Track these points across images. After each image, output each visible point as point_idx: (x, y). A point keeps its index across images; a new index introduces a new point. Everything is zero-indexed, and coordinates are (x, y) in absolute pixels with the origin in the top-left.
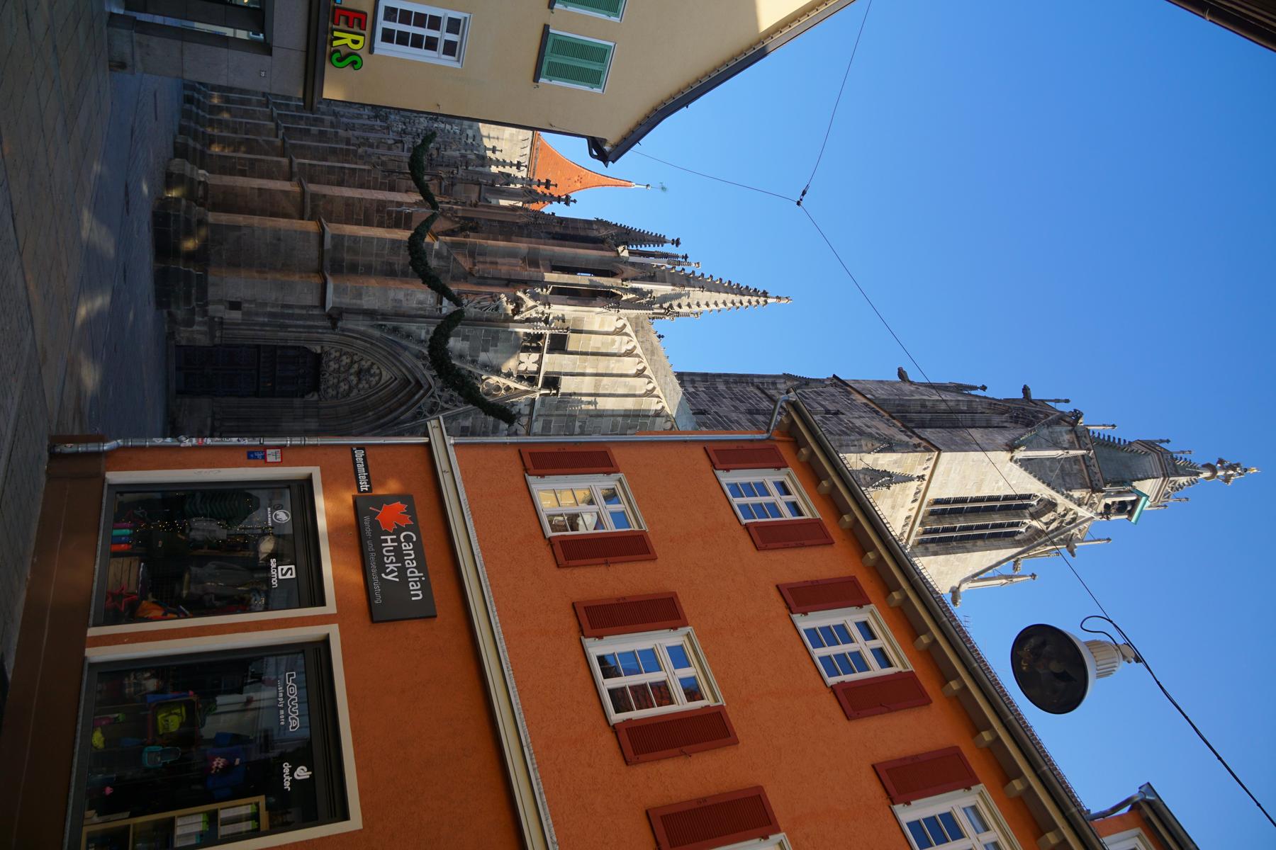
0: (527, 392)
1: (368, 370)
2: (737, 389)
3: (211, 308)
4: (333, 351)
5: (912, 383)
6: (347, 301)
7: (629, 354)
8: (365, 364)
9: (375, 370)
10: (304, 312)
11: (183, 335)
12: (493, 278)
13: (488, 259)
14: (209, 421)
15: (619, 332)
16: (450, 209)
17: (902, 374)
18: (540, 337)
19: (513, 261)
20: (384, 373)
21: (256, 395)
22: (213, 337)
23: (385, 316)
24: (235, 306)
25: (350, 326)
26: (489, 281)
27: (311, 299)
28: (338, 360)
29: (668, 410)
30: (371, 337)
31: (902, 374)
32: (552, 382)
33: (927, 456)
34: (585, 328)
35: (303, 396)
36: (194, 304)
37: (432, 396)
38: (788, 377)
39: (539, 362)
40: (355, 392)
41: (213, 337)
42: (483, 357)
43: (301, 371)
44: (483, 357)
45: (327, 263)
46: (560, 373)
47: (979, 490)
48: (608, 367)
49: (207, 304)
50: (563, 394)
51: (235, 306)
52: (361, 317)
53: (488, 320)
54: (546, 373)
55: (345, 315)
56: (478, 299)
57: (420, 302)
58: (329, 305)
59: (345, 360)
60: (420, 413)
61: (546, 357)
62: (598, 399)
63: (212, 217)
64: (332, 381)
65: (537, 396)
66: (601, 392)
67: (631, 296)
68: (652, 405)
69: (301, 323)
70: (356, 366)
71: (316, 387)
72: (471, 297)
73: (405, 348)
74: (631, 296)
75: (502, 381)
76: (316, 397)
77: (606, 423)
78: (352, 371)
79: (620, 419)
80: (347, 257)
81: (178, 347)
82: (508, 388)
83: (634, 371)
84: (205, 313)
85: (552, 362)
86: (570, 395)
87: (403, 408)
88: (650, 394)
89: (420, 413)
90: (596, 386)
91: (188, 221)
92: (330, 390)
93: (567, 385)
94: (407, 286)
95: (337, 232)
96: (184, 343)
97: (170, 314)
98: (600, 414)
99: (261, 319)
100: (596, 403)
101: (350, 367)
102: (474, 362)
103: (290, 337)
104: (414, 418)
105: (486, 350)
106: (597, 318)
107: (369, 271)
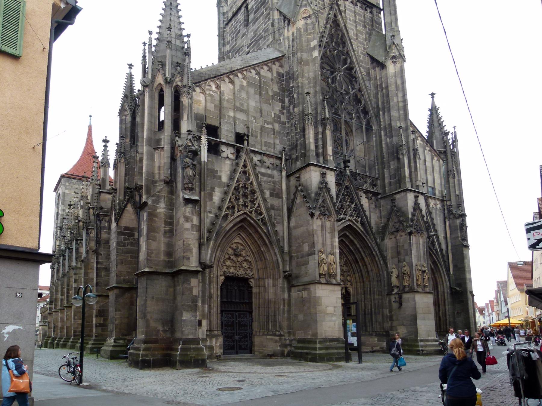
1: (234, 250)
2: (228, 38)
8: (231, 252)
9: (234, 246)
11: (218, 351)
20: (236, 241)
28: (228, 267)
37: (251, 212)
40: (247, 258)
59: (228, 263)
60: (262, 220)
70: (232, 257)
78: (235, 259)
84: (204, 340)
87: (259, 230)
89: (262, 220)
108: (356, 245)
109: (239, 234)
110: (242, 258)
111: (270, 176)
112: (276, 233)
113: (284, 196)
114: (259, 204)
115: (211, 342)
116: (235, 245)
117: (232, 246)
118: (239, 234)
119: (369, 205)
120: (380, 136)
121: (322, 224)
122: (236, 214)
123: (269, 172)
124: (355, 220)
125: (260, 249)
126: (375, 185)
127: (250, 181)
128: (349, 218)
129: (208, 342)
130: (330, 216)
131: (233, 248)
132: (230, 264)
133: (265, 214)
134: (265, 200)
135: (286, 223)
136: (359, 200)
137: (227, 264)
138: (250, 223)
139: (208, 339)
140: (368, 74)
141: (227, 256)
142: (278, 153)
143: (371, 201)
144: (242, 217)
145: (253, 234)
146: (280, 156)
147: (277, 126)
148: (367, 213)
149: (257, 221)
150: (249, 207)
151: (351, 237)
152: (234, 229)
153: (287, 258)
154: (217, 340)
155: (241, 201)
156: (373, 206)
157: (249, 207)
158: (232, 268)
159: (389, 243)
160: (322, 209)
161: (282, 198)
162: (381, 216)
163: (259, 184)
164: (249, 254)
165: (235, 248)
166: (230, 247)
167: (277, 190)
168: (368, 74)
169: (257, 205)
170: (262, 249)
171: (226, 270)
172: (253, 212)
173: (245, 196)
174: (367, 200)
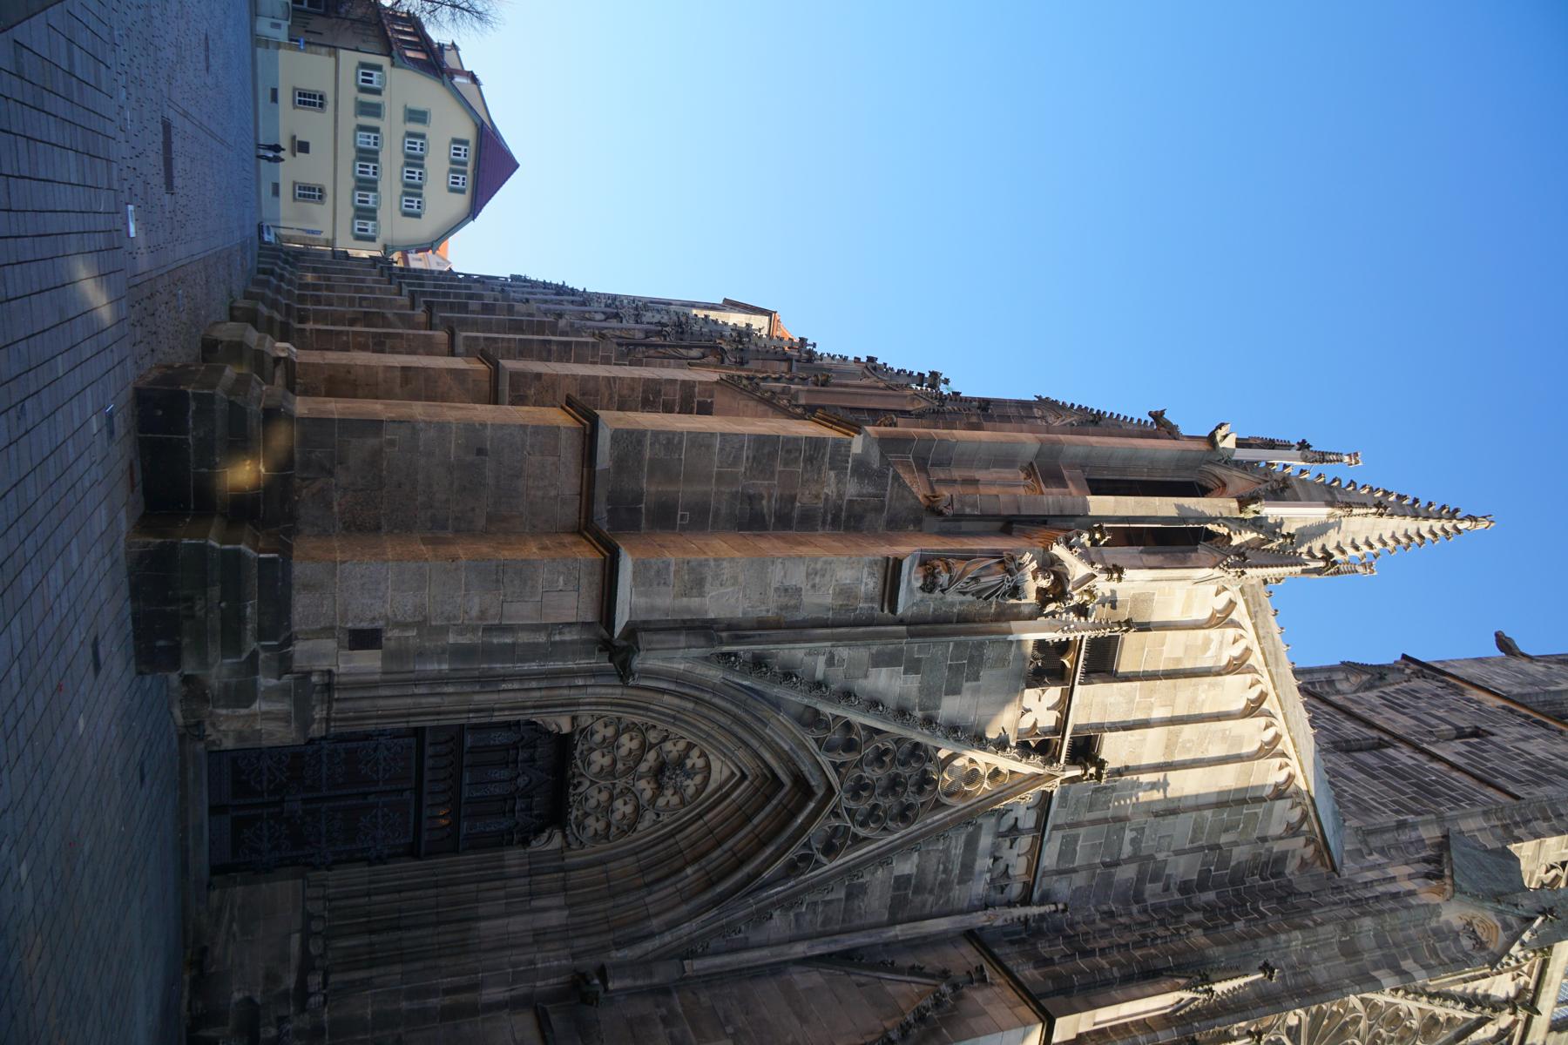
0: (1036, 778)
1: (680, 762)
3: (299, 647)
5: (1531, 659)
6: (668, 602)
7: (1237, 666)
8: (673, 749)
9: (695, 760)
10: (542, 638)
11: (227, 727)
12: (983, 517)
13: (957, 474)
15: (1222, 619)
16: (784, 391)
17: (1504, 643)
18: (1063, 647)
19: (1007, 474)
20: (716, 765)
21: (413, 852)
22: (305, 724)
23: (737, 630)
24: (364, 639)
26: (965, 526)
27: (571, 604)
28: (611, 745)
29: (1300, 783)
30: (699, 685)
31: (1504, 643)
32: (1085, 749)
34: (1156, 617)
35: (525, 842)
36: (251, 644)
38: (1350, 667)
39: (1064, 706)
41: (305, 724)
42: (950, 707)
43: (522, 781)
45: (601, 509)
46: (1102, 728)
48: (1193, 701)
49: (289, 641)
51: (364, 639)
52: (682, 639)
53: (963, 619)
54: (1076, 729)
55: (643, 637)
56: (973, 569)
57: (846, 592)
58: (622, 619)
59: (628, 743)
61: (1077, 688)
62: (1172, 776)
63: (302, 406)
64: (597, 797)
66: (1178, 757)
67: (1249, 536)
68: (1269, 774)
69: (534, 666)
71: (556, 815)
72: (958, 567)
74: (1249, 536)
75: (984, 760)
76: (557, 841)
77: (1181, 829)
78: (643, 767)
79: (1208, 813)
80: (650, 488)
81: (216, 755)
82: (996, 773)
83: (1240, 705)
84: (284, 664)
85: (1094, 702)
86: (1119, 772)
87: (769, 851)
90: (1169, 746)
91: (237, 415)
92: (590, 821)
93: (1114, 750)
94: (803, 550)
95: (620, 426)
96: (229, 744)
98: (1172, 809)
99: (433, 667)
100: (1164, 785)
102: (929, 721)
103: (502, 702)
106: (1177, 593)
107: (701, 519)
109: (744, 777)
110: (648, 794)
114: (865, 839)
115: (270, 694)
116: (700, 763)
117: (695, 753)
118: (744, 777)
125: (688, 864)
127: (945, 800)
129: (273, 682)
131: (687, 756)
132: (623, 751)
133: (831, 865)
134: (883, 859)
138: (793, 815)
139: (286, 678)
141: (653, 737)
142: (1044, 887)
145: (749, 828)
149: (804, 839)
150: (852, 805)
152: (767, 756)
154: (285, 718)
155: (872, 774)
157: (852, 805)
158: (607, 761)
163: (939, 832)
164: (665, 818)
165: (689, 763)
166: (690, 746)
167: (918, 900)
169: (862, 832)
170: (689, 871)
171: (598, 738)
172: (835, 823)
173: (894, 784)
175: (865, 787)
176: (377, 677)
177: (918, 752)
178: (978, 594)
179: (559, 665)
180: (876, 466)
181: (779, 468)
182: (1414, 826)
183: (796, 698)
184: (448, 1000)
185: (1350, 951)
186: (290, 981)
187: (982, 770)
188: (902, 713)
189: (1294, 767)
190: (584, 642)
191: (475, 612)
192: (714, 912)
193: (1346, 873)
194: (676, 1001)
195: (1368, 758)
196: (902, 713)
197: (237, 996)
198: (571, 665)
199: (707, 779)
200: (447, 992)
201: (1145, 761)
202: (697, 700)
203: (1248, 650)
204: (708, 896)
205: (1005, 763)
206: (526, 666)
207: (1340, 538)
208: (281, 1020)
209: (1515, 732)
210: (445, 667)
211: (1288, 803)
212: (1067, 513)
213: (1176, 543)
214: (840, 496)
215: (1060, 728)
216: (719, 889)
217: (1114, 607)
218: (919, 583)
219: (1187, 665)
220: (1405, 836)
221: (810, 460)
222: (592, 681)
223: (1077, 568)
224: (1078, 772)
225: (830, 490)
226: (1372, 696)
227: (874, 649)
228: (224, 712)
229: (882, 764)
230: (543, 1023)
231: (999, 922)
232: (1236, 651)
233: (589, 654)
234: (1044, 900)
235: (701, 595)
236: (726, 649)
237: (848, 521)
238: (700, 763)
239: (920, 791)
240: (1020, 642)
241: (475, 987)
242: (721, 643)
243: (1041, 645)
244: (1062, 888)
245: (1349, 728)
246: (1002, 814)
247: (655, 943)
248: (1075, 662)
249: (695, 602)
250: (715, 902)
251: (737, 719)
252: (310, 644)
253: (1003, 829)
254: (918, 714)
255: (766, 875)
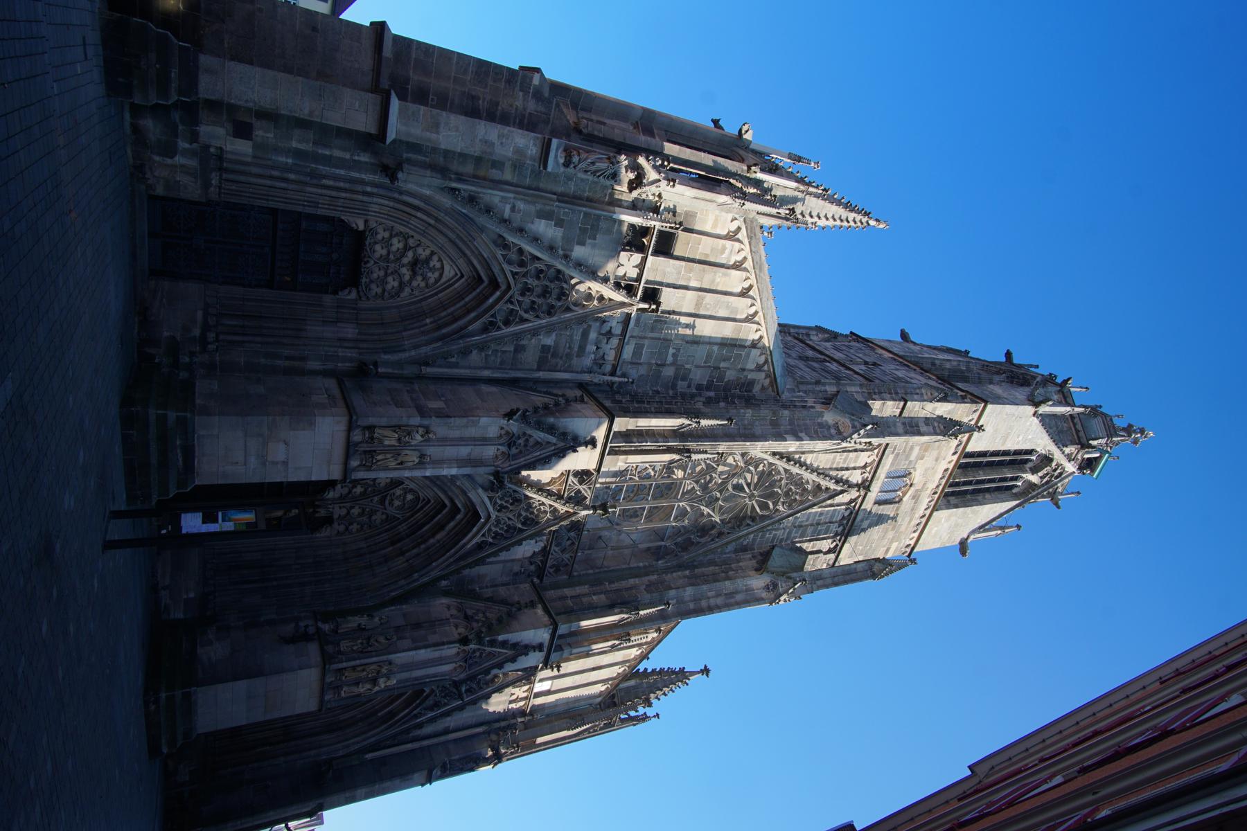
0: (623, 305)
4: (380, 230)
5: (915, 344)
6: (417, 132)
7: (738, 266)
8: (423, 253)
9: (434, 262)
13: (594, 117)
14: (200, 314)
15: (732, 237)
17: (904, 335)
18: (645, 231)
19: (623, 125)
20: (447, 268)
22: (206, 185)
25: (411, 187)
28: (387, 243)
29: (765, 341)
31: (904, 335)
32: (652, 295)
33: (974, 407)
34: (696, 228)
35: (335, 293)
37: (510, 301)
38: (819, 329)
39: (641, 266)
40: (407, 290)
41: (206, 185)
42: (579, 252)
44: (579, 252)
46: (661, 284)
47: (1004, 443)
48: (713, 281)
50: (663, 312)
52: (428, 173)
53: (589, 200)
54: (647, 282)
55: (406, 166)
57: (519, 151)
58: (391, 136)
60: (492, 324)
61: (650, 258)
62: (698, 321)
64: (377, 273)
65: (633, 311)
66: (702, 312)
68: (750, 333)
69: (342, 172)
70: (410, 254)
72: (584, 155)
73: (482, 229)
75: (596, 287)
76: (353, 295)
77: (700, 353)
78: (405, 261)
80: (415, 77)
81: (153, 198)
82: (601, 298)
83: (738, 290)
84: (194, 137)
85: (658, 268)
86: (669, 313)
87: (473, 315)
88: (750, 319)
90: (698, 304)
92: (373, 286)
93: (669, 299)
96: (160, 191)
97: (136, 129)
98: (696, 341)
99: (282, 159)
100: (692, 327)
101: (403, 255)
104: (485, 330)
105: (582, 243)
107: (443, 103)
108: (433, 535)
109: (462, 276)
110: (407, 277)
111: (582, 348)
112: (465, 352)
113: (541, 374)
116: (438, 265)
117: (435, 258)
118: (462, 276)
119: (519, 560)
120: (647, 574)
121: (490, 439)
122: (505, 266)
123: (591, 348)
124: (490, 530)
126: (557, 570)
128: (493, 517)
129: (187, 146)
130: (507, 456)
132: (394, 248)
134: (535, 332)
135: (486, 373)
136: (530, 537)
137: (395, 241)
138: (487, 298)
140: (744, 549)
143: (527, 562)
144: (500, 279)
145: (462, 303)
146: (618, 373)
147: (669, 372)
148: (504, 556)
149: (492, 312)
150: (521, 299)
151: (452, 524)
153: (409, 371)
155: (532, 282)
156: (516, 568)
157: (521, 299)
159: (441, 605)
160: (521, 441)
161: (539, 369)
162: (496, 586)
164: (416, 293)
165: (432, 264)
166: (433, 253)
168: (744, 549)
170: (428, 321)
173: (545, 293)
174: (529, 554)
175: (529, 290)
176: (249, 160)
177: (559, 276)
178: (594, 173)
179: (357, 175)
180: (546, 95)
181: (490, 82)
182: (824, 384)
183: (494, 227)
184: (287, 363)
185: (774, 424)
186: (197, 332)
187: (594, 294)
188: (551, 249)
189: (763, 332)
190: (372, 164)
191: (306, 111)
192: (439, 344)
193: (784, 397)
194: (416, 387)
195: (815, 365)
196: (551, 249)
197: (166, 334)
198: (363, 176)
199: (441, 275)
200: (287, 358)
201: (684, 310)
202: (437, 219)
203: (745, 258)
204: (436, 334)
205: (609, 293)
206: (338, 171)
207: (803, 208)
208: (192, 354)
209: (893, 367)
210: (290, 161)
211: (758, 352)
212: (652, 148)
213: (710, 181)
214: (525, 109)
215: (639, 279)
216: (444, 331)
217: (674, 215)
218: (562, 161)
219: (712, 259)
220: (818, 388)
221: (508, 82)
222: (375, 190)
223: (652, 175)
224: (646, 306)
225: (519, 103)
226: (828, 345)
227: (539, 207)
228: (157, 158)
229: (538, 278)
230: (340, 384)
231: (596, 381)
232: (739, 258)
233: (375, 173)
234: (624, 375)
235: (438, 133)
236: (454, 185)
237: (527, 123)
238: (438, 265)
239: (559, 299)
240: (621, 222)
241: (303, 359)
242: (450, 179)
243: (632, 226)
244: (634, 373)
245: (810, 353)
246: (604, 321)
247: (407, 354)
248: (651, 242)
249: (434, 136)
250: (442, 338)
251: (461, 239)
252: (209, 128)
253: (603, 332)
254: (561, 252)
255: (470, 328)
